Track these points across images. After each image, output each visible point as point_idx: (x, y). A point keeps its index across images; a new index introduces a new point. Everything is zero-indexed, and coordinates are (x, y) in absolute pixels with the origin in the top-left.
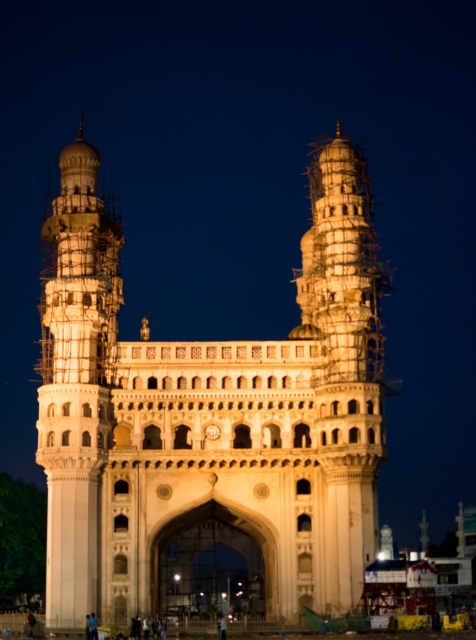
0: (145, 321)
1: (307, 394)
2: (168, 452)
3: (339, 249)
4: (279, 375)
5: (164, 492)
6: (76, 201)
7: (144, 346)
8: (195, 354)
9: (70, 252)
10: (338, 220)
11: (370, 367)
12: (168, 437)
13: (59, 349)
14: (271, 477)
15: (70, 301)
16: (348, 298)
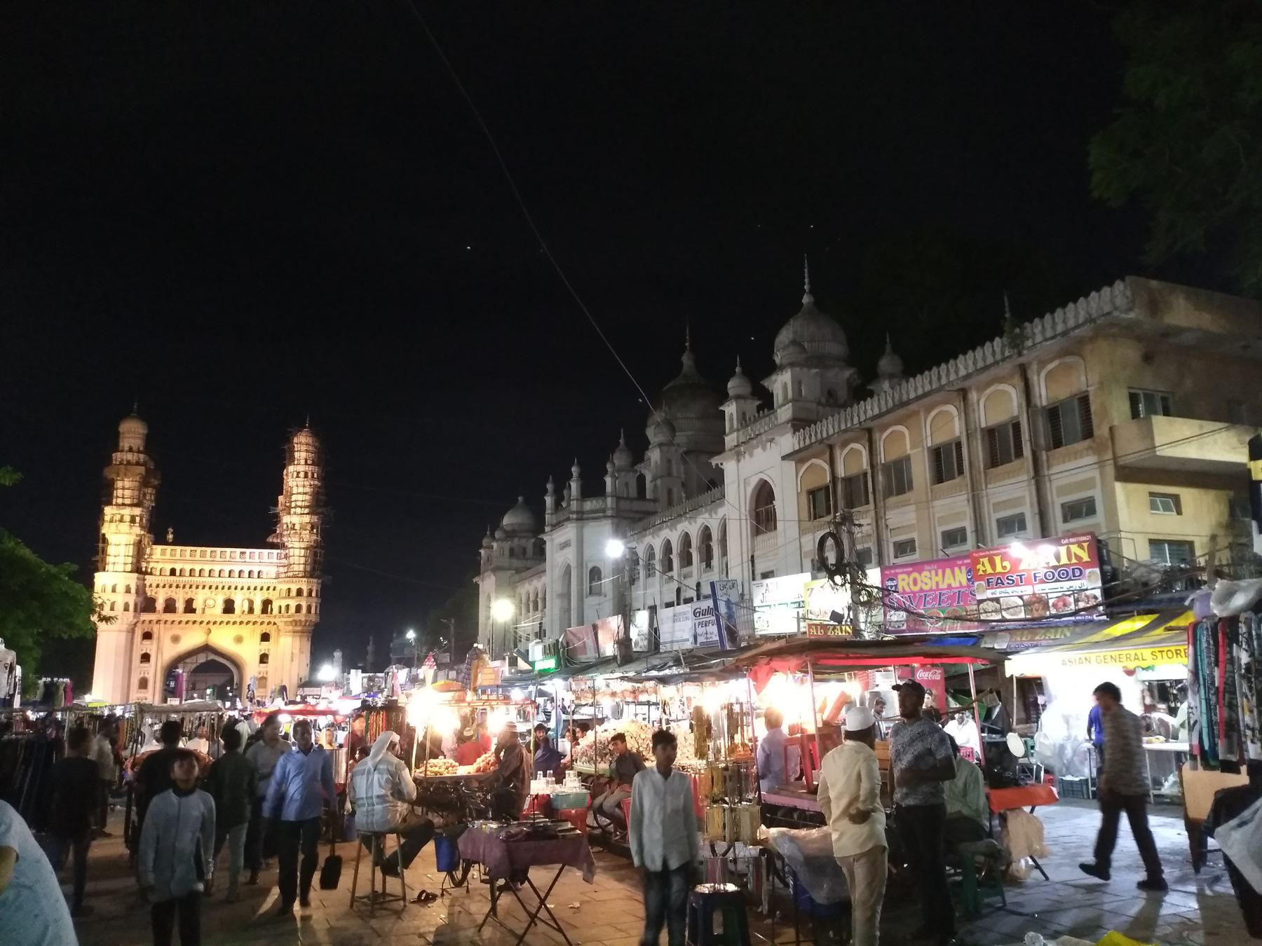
0: (171, 530)
1: (272, 583)
2: (180, 615)
3: (300, 497)
4: (256, 570)
5: (176, 639)
6: (129, 456)
7: (169, 548)
8: (203, 554)
9: (123, 489)
10: (301, 481)
11: (313, 569)
12: (180, 606)
13: (111, 550)
14: (245, 631)
15: (121, 520)
16: (303, 528)
